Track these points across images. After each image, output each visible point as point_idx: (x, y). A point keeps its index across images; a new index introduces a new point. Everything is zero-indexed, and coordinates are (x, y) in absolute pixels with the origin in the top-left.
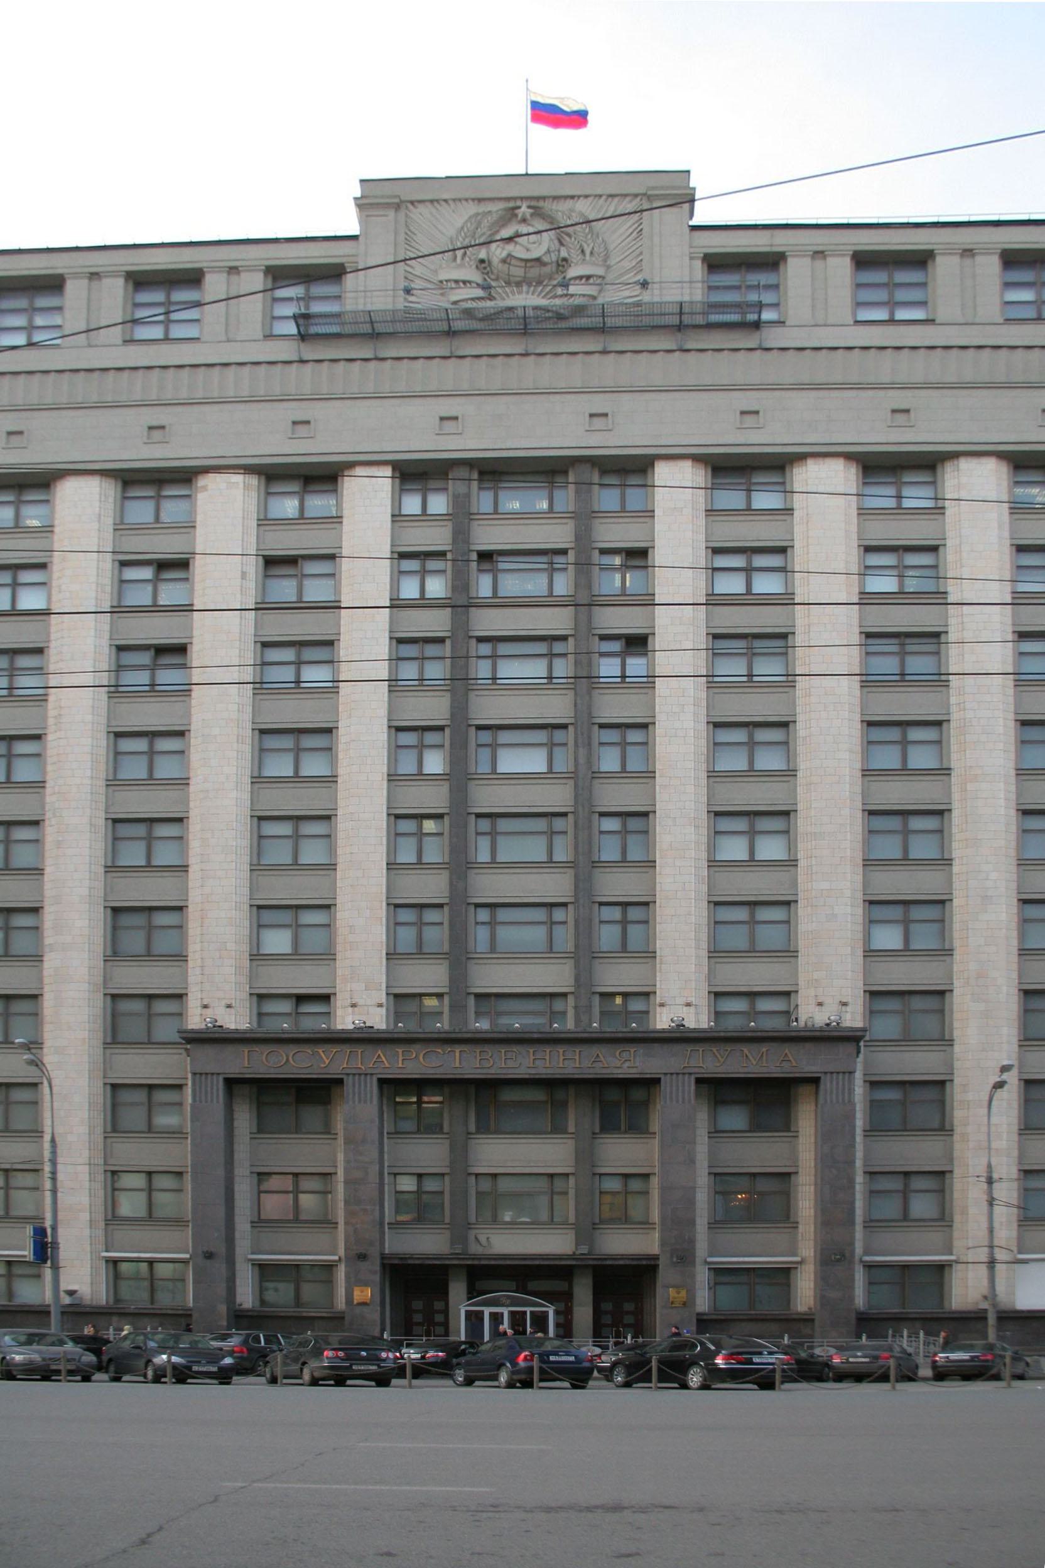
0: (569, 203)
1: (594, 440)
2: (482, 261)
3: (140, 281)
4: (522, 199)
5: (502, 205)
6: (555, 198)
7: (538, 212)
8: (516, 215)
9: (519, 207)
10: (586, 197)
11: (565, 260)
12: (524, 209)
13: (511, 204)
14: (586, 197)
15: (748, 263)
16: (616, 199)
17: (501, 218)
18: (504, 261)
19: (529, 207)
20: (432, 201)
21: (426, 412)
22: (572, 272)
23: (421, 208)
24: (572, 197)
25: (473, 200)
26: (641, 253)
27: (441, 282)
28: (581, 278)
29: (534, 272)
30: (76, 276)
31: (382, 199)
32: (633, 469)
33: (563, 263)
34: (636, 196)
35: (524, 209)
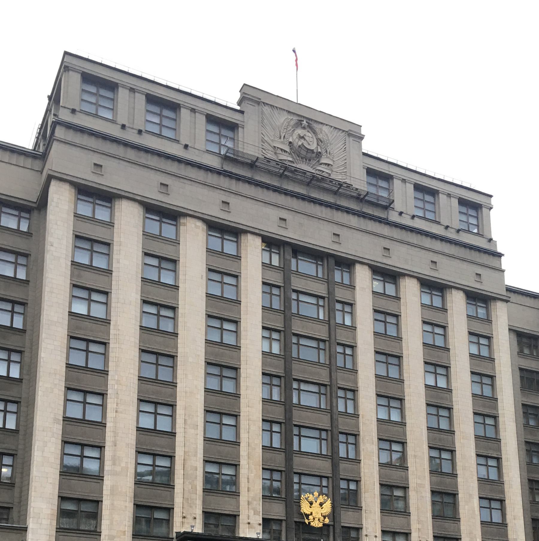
0: (321, 126)
1: (335, 247)
2: (290, 143)
3: (151, 99)
4: (304, 117)
5: (298, 118)
6: (316, 121)
7: (310, 127)
8: (301, 124)
9: (303, 121)
10: (327, 125)
11: (320, 153)
12: (305, 122)
13: (300, 119)
14: (327, 125)
15: (381, 173)
16: (337, 130)
17: (297, 123)
18: (299, 146)
19: (307, 122)
20: (271, 105)
21: (274, 214)
22: (323, 161)
23: (266, 107)
24: (322, 123)
25: (287, 111)
26: (346, 159)
27: (275, 147)
28: (326, 164)
29: (309, 155)
30: (124, 87)
31: (250, 96)
32: (347, 264)
33: (319, 155)
34: (344, 131)
35: (305, 122)
